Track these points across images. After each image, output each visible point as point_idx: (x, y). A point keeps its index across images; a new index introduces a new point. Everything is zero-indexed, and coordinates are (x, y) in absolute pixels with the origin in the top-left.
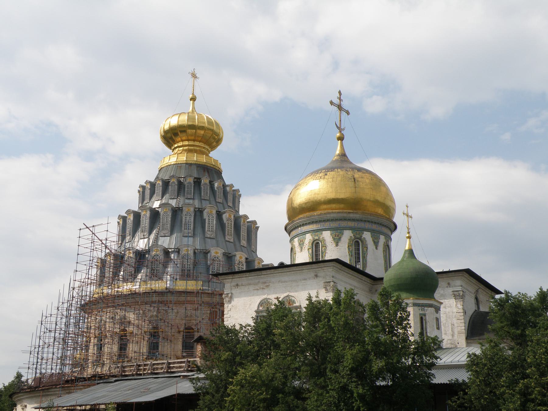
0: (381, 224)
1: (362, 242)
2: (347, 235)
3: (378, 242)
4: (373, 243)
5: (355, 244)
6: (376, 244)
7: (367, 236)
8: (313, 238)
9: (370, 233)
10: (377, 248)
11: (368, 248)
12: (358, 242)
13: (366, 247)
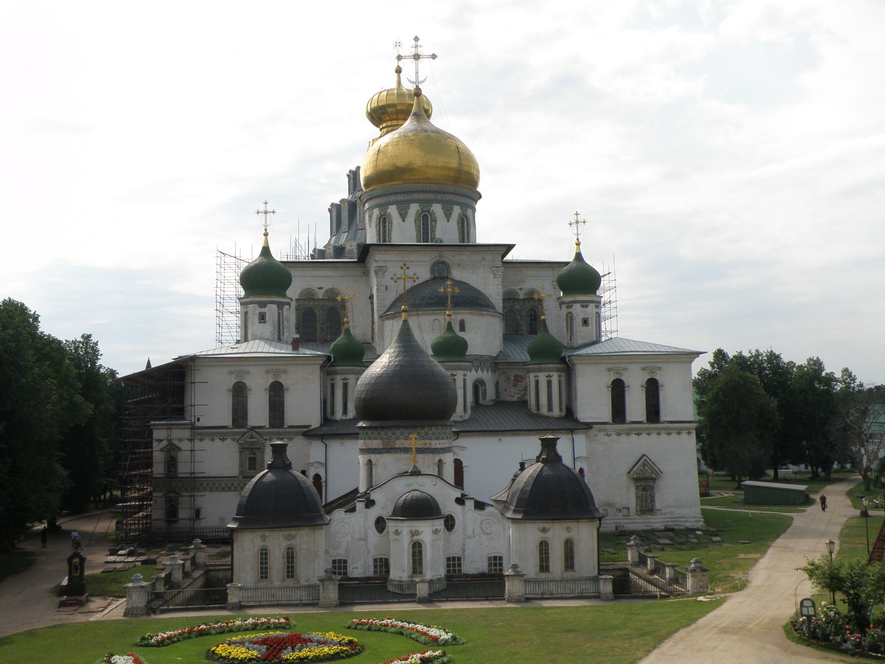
0: (459, 194)
2: (414, 208)
3: (451, 214)
4: (444, 215)
5: (423, 218)
6: (448, 215)
7: (437, 209)
8: (380, 213)
9: (440, 205)
10: (448, 221)
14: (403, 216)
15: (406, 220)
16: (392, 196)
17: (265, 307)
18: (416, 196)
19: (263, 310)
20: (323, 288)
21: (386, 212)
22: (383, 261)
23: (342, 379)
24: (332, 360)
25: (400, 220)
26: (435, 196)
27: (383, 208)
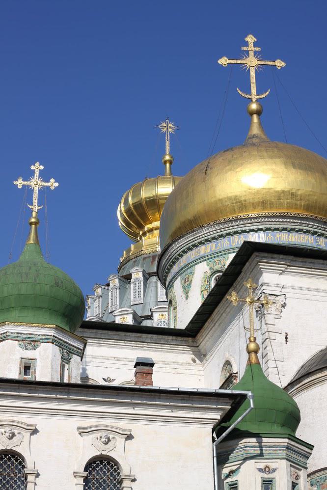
17: (34, 348)
19: (29, 354)
20: (114, 380)
22: (277, 286)
23: (260, 470)
24: (252, 406)
27: (217, 259)
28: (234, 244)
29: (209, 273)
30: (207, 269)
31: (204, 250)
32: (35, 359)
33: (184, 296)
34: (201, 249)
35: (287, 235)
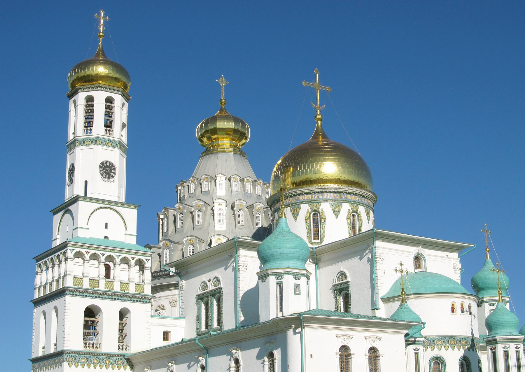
1: (358, 215)
2: (346, 208)
9: (364, 207)
11: (363, 221)
12: (353, 216)
13: (360, 220)
14: (337, 213)
15: (338, 216)
16: (325, 194)
18: (348, 197)
19: (297, 282)
21: (319, 208)
23: (414, 349)
25: (335, 216)
26: (361, 199)
27: (315, 204)
28: (324, 198)
29: (310, 210)
30: (309, 208)
31: (307, 197)
32: (300, 284)
33: (294, 219)
34: (305, 196)
35: (350, 196)
